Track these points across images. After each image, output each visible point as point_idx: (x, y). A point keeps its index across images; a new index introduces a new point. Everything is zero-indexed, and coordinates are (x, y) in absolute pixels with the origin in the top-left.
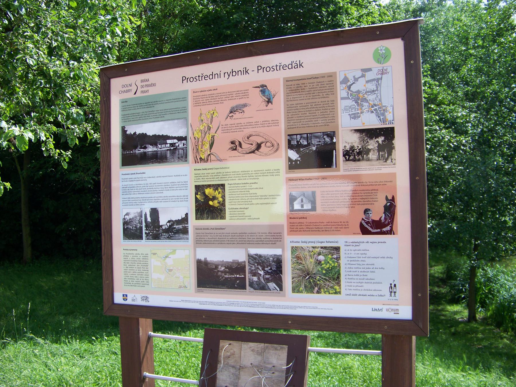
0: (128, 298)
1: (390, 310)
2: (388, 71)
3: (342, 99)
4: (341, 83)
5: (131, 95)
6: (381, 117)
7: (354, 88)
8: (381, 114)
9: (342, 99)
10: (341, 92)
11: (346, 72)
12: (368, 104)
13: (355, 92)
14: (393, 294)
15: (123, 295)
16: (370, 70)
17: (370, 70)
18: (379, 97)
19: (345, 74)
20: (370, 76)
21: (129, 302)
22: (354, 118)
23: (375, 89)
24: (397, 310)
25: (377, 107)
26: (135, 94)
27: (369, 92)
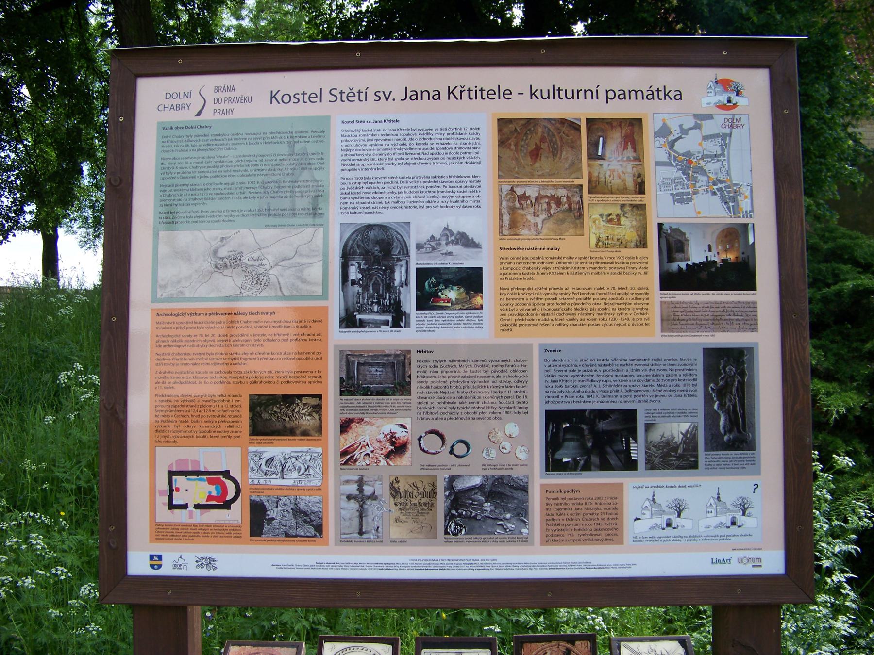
0: (164, 562)
1: (745, 561)
2: (742, 123)
3: (658, 164)
4: (656, 135)
5: (188, 116)
6: (731, 204)
8: (730, 197)
9: (658, 164)
11: (666, 117)
12: (705, 178)
13: (683, 155)
15: (152, 557)
16: (710, 117)
17: (710, 117)
18: (726, 167)
19: (664, 120)
20: (710, 128)
23: (719, 152)
24: (759, 559)
25: (722, 186)
26: (199, 114)
27: (707, 156)
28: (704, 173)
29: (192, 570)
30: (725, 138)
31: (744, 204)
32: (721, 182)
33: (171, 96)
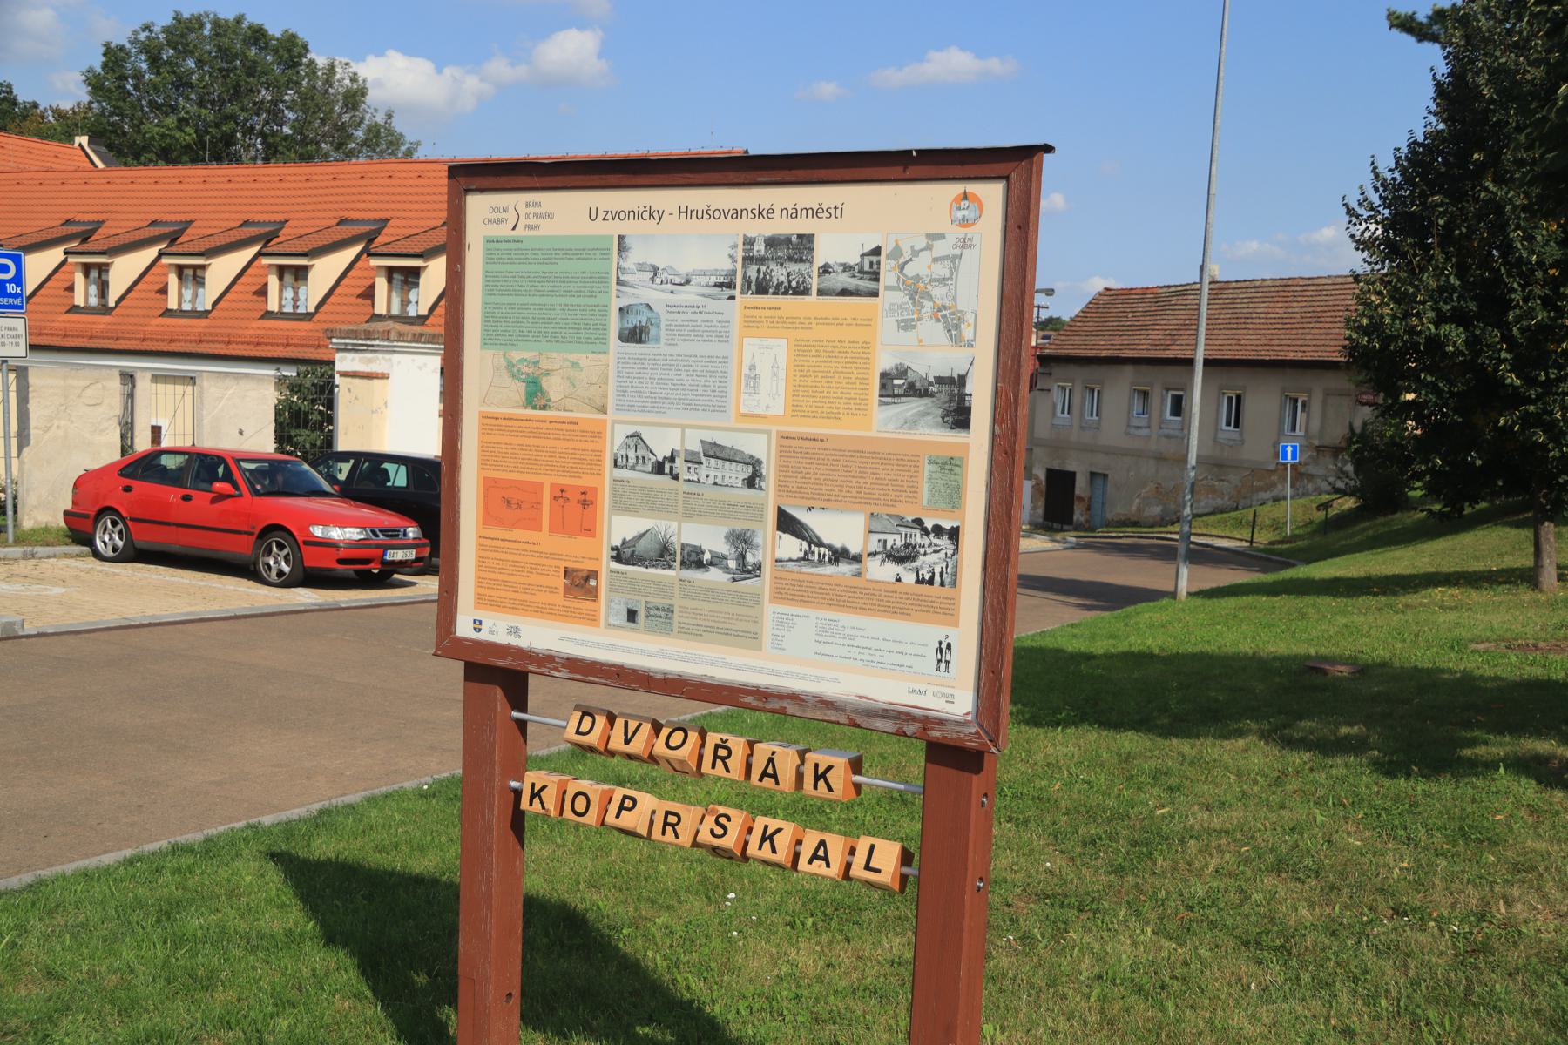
5: (504, 231)
7: (910, 270)
14: (943, 665)
16: (941, 236)
17: (941, 236)
20: (941, 248)
21: (484, 636)
22: (905, 328)
27: (936, 280)
28: (931, 298)
29: (502, 638)
30: (955, 259)
31: (967, 332)
32: (945, 308)
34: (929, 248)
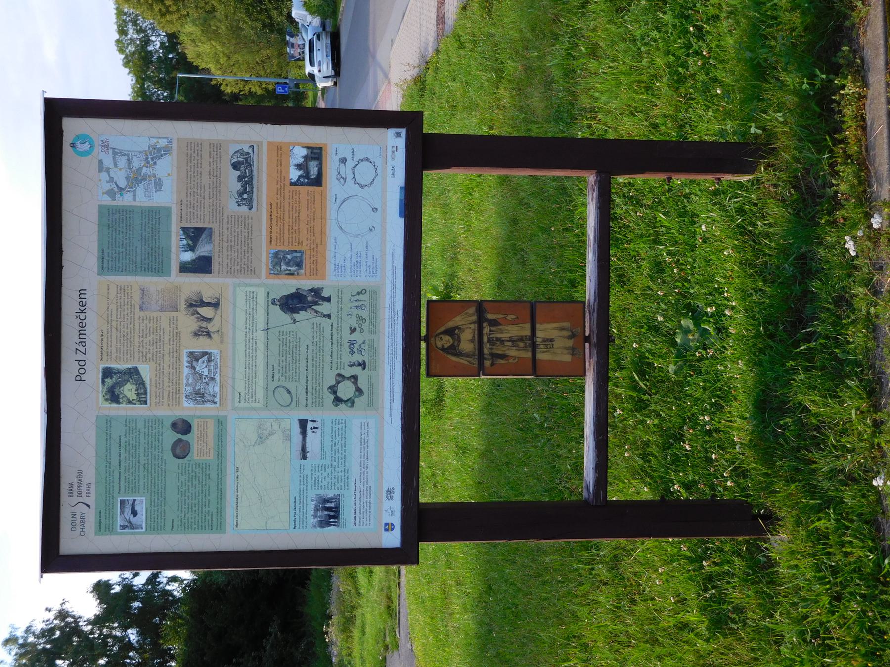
0: (389, 522)
3: (134, 199)
7: (122, 183)
9: (134, 199)
10: (126, 200)
15: (386, 530)
16: (101, 162)
20: (108, 161)
21: (397, 520)
24: (393, 147)
26: (88, 506)
28: (141, 168)
30: (115, 152)
31: (162, 143)
33: (74, 526)
34: (108, 171)
